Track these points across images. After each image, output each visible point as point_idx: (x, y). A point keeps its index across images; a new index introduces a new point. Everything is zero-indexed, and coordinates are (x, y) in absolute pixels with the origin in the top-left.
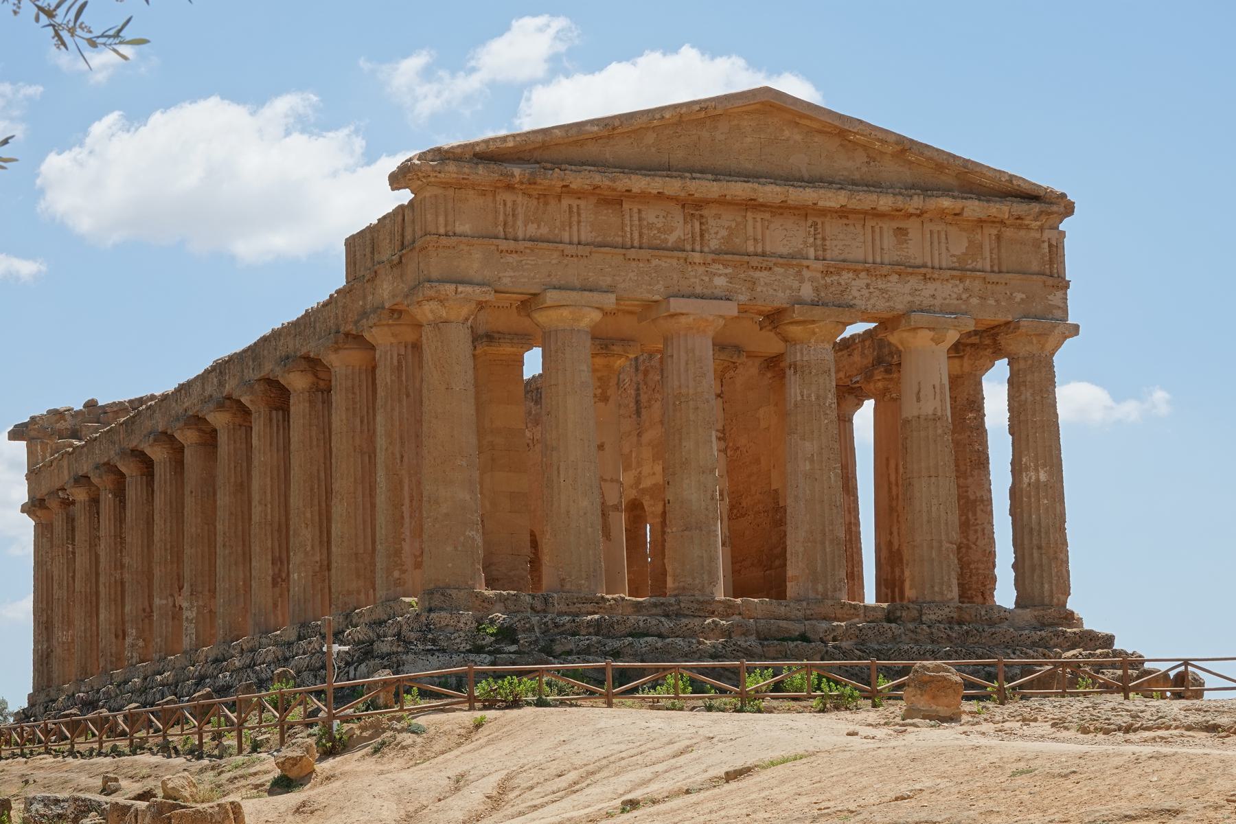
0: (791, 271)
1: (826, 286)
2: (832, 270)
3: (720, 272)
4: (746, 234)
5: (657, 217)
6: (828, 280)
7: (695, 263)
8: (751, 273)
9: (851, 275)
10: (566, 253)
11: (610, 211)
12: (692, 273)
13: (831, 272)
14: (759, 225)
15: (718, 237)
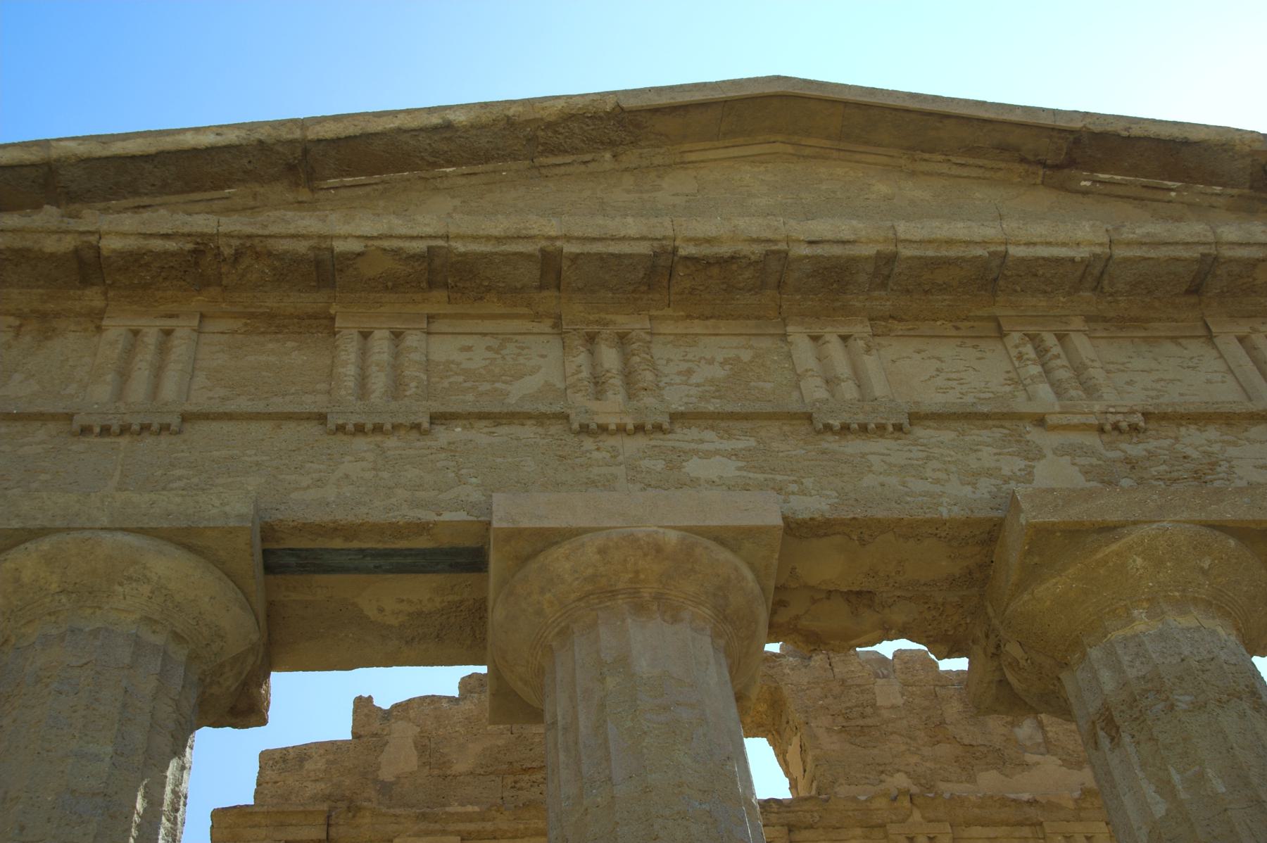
0: (985, 435)
1: (1131, 463)
2: (1138, 419)
3: (705, 446)
4: (794, 369)
5: (469, 349)
6: (1135, 450)
7: (603, 429)
8: (831, 443)
9: (1212, 433)
10: (80, 420)
11: (290, 344)
12: (596, 455)
13: (1134, 428)
14: (834, 348)
15: (695, 379)
